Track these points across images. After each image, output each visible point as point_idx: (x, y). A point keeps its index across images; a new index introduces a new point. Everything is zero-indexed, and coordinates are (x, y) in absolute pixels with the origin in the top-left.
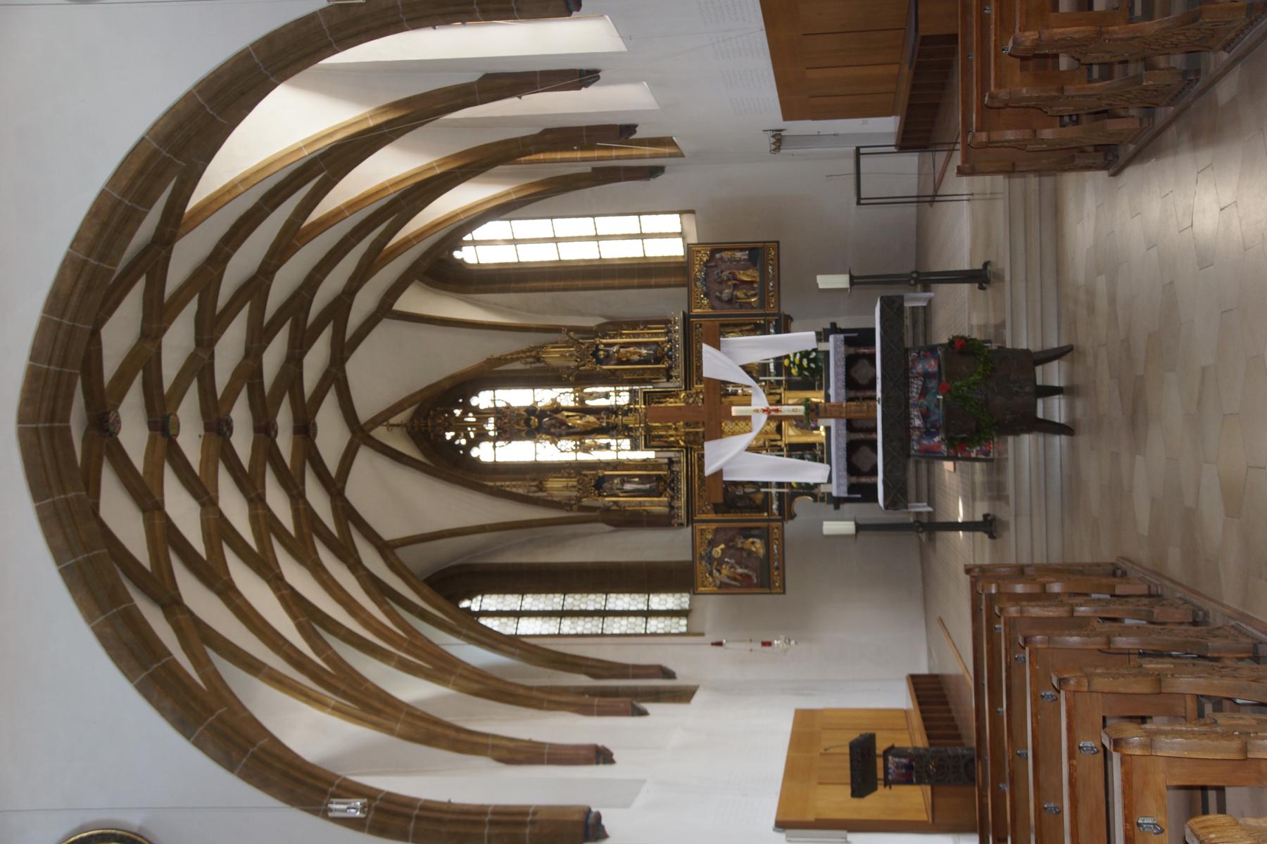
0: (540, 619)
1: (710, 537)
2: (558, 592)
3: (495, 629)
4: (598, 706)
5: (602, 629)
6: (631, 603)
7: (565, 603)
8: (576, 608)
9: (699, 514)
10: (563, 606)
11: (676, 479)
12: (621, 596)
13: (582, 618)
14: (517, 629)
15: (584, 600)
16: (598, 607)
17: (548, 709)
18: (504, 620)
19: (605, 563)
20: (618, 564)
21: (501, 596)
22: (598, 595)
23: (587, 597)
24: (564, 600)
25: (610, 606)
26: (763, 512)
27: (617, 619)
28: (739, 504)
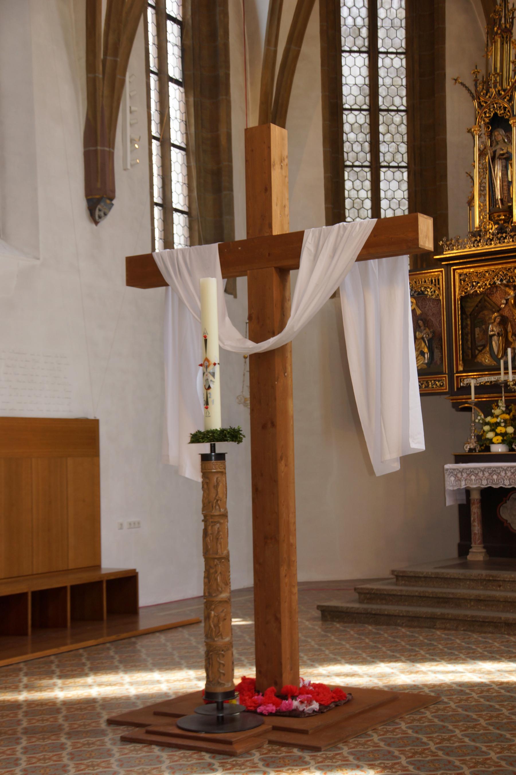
0: (367, 82)
1: (429, 292)
2: (407, 101)
3: (350, 21)
4: (96, 151)
5: (353, 166)
6: (394, 200)
7: (393, 113)
8: (382, 129)
9: (460, 275)
10: (388, 110)
11: (504, 235)
12: (405, 186)
13: (368, 137)
14: (351, 52)
15: (398, 138)
16: (388, 157)
17: (88, 79)
18: (364, 32)
19: (445, 158)
20: (444, 177)
21: (404, 24)
22: (405, 156)
23: (403, 142)
24: (398, 111)
25: (385, 174)
26: (464, 366)
27: (367, 184)
28: (477, 330)
